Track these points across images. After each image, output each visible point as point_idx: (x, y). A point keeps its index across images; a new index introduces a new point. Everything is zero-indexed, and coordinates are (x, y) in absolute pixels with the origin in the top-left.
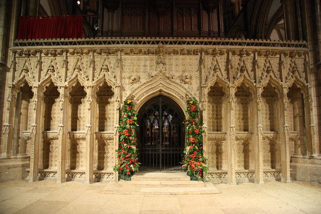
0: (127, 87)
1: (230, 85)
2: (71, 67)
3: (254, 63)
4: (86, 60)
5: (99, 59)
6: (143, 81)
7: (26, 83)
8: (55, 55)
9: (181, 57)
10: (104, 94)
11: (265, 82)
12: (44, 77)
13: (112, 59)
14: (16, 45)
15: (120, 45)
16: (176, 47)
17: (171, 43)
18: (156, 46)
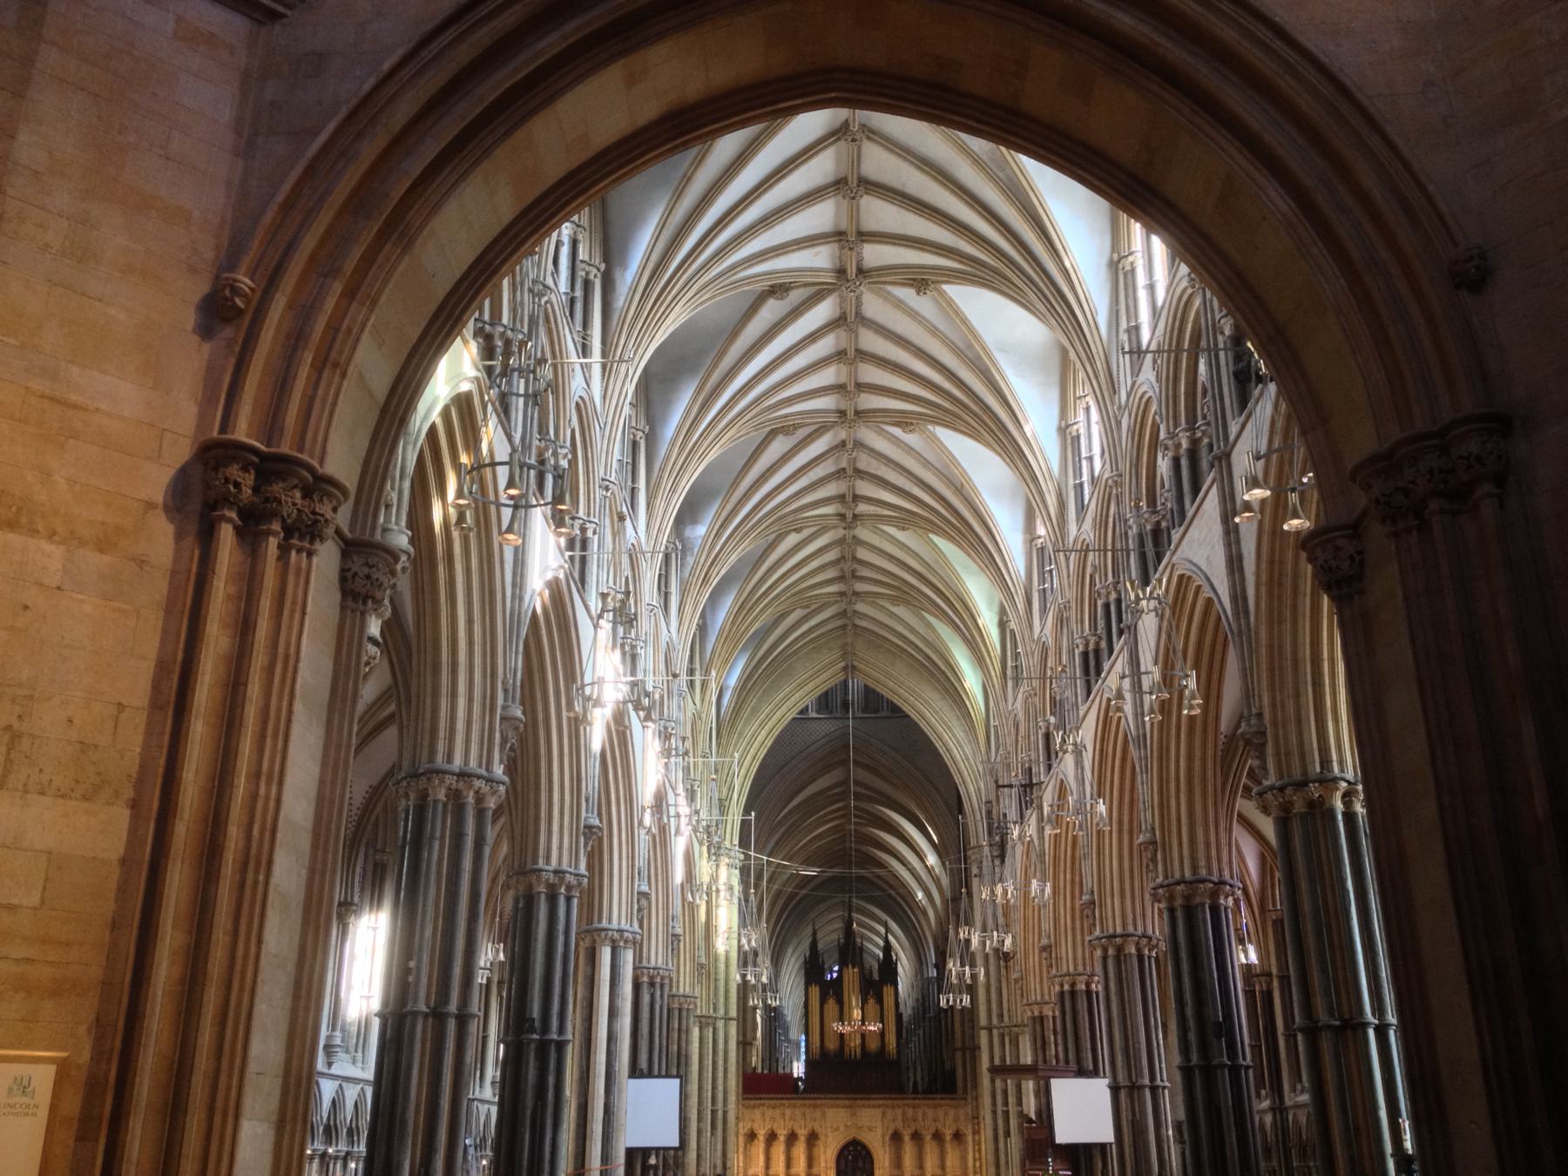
0: (830, 1135)
1: (905, 1132)
2: (787, 1117)
3: (924, 1114)
4: (798, 1112)
5: (807, 1111)
6: (842, 1129)
7: (752, 1132)
8: (774, 1108)
9: (868, 1110)
10: (812, 1138)
11: (932, 1130)
12: (768, 1127)
13: (818, 1113)
14: (744, 1099)
15: (824, 1102)
16: (863, 1102)
17: (861, 1099)
18: (847, 1102)
